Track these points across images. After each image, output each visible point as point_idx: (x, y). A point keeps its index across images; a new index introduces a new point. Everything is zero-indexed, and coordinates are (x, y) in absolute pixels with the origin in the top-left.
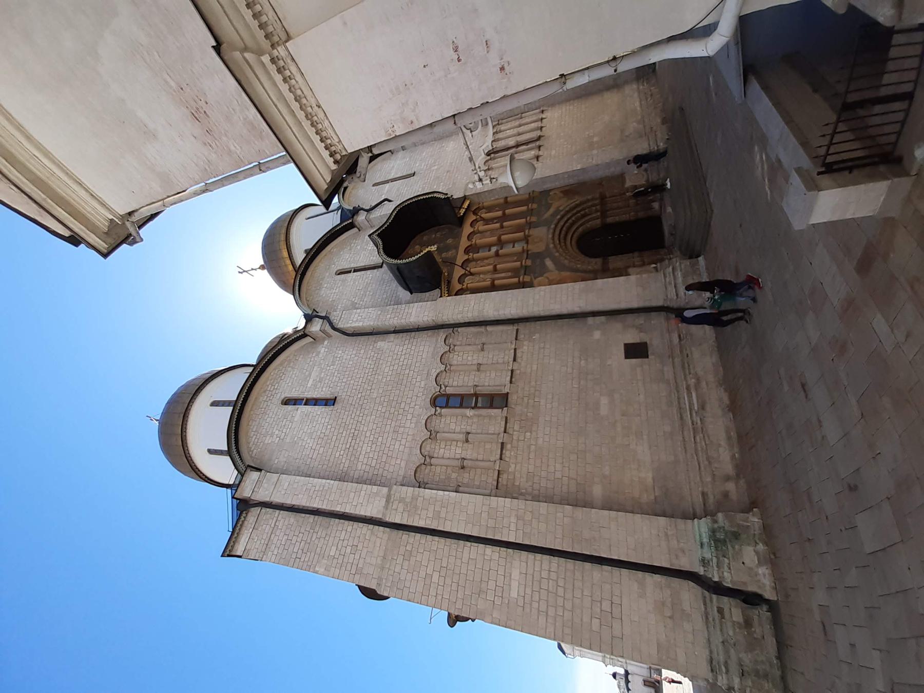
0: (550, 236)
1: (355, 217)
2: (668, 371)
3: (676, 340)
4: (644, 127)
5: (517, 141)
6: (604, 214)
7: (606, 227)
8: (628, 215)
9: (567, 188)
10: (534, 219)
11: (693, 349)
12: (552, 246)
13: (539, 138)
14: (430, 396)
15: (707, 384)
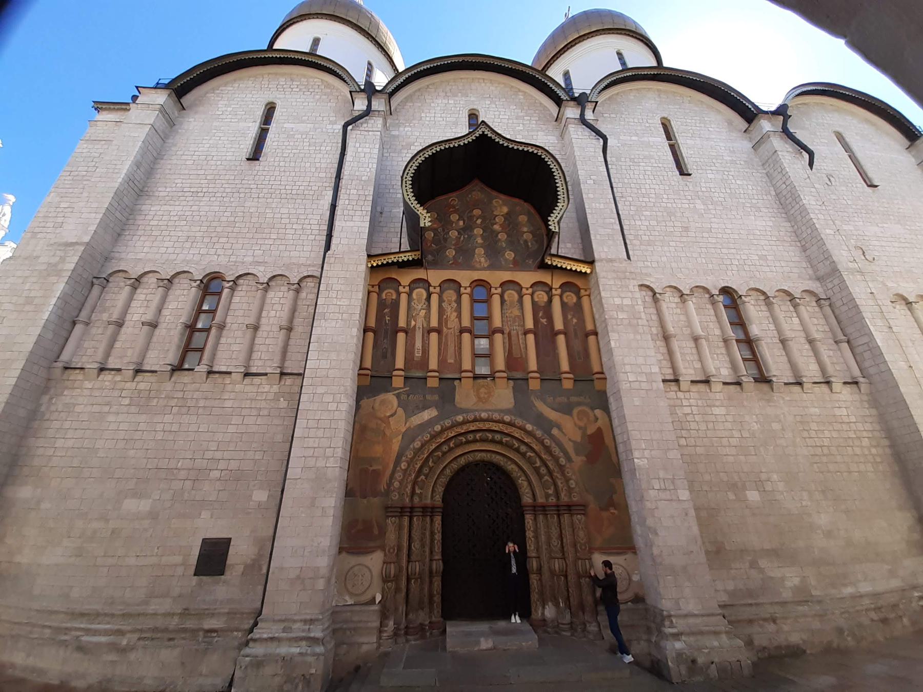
0: (484, 415)
1: (572, 103)
2: (165, 605)
3: (210, 624)
4: (784, 604)
5: (758, 340)
6: (539, 509)
7: (520, 511)
8: (534, 555)
9: (608, 440)
10: (534, 385)
11: (176, 652)
12: (460, 418)
13: (763, 379)
14: (221, 271)
15: (113, 662)
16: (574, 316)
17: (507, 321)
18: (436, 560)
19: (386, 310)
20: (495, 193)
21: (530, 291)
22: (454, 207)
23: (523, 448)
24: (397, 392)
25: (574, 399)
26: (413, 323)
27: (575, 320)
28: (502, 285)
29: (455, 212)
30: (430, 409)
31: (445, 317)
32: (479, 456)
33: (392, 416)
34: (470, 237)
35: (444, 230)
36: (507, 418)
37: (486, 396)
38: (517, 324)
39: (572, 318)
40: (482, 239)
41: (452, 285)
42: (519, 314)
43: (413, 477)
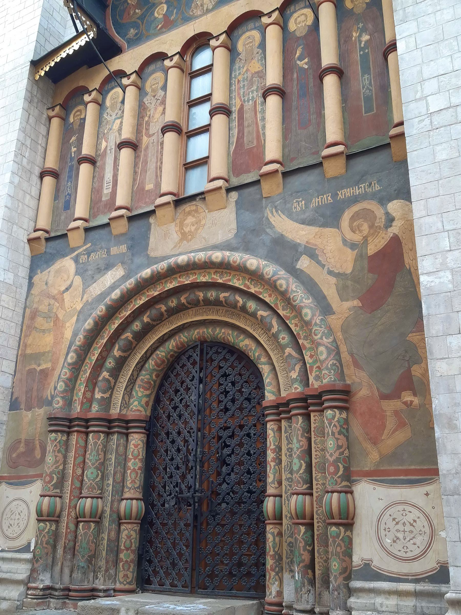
0: (182, 259)
17: (239, 88)
18: (127, 499)
23: (252, 305)
24: (76, 253)
26: (104, 144)
30: (114, 269)
31: (146, 119)
32: (196, 333)
33: (67, 289)
36: (217, 256)
37: (193, 228)
38: (255, 88)
43: (88, 374)
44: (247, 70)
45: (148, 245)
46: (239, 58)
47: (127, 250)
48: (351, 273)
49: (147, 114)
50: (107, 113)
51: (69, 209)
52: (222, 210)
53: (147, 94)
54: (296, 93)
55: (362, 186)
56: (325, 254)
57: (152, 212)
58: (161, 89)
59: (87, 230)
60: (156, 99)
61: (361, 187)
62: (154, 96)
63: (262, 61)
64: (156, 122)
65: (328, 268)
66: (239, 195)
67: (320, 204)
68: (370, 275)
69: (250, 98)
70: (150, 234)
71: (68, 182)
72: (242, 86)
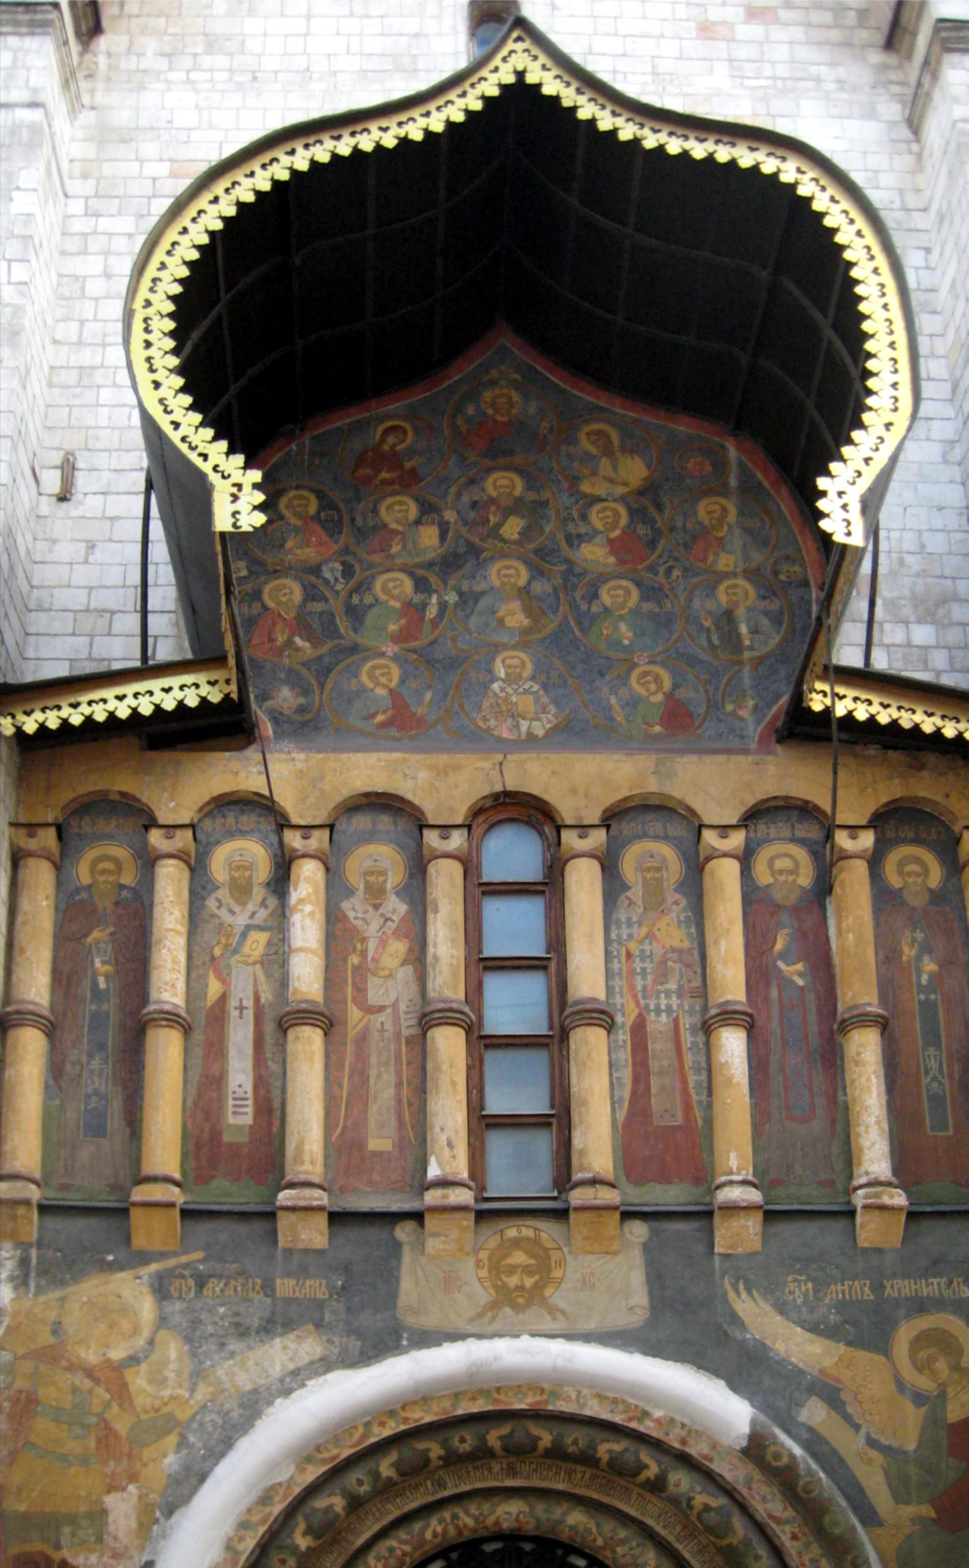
16: (926, 948)
17: (632, 973)
19: (96, 934)
20: (586, 395)
21: (737, 840)
22: (394, 461)
24: (154, 1267)
25: (900, 1288)
26: (214, 988)
27: (929, 966)
28: (611, 818)
29: (408, 481)
30: (292, 1336)
31: (355, 959)
34: (468, 599)
35: (348, 571)
37: (529, 1282)
38: (673, 986)
39: (919, 958)
40: (528, 611)
41: (385, 821)
42: (686, 944)
44: (651, 936)
45: (393, 1296)
46: (628, 898)
47: (331, 1296)
48: (916, 1450)
49: (355, 949)
50: (218, 900)
51: (104, 1136)
52: (609, 1257)
53: (350, 892)
54: (779, 1035)
55: (935, 1281)
56: (860, 1402)
57: (418, 1217)
58: (398, 894)
59: (186, 1214)
60: (382, 915)
61: (932, 1284)
62: (376, 907)
63: (688, 927)
64: (386, 977)
65: (868, 1433)
66: (654, 1233)
67: (847, 1297)
68: (953, 1462)
69: (663, 1007)
70: (398, 1268)
71: (91, 1056)
72: (638, 970)
